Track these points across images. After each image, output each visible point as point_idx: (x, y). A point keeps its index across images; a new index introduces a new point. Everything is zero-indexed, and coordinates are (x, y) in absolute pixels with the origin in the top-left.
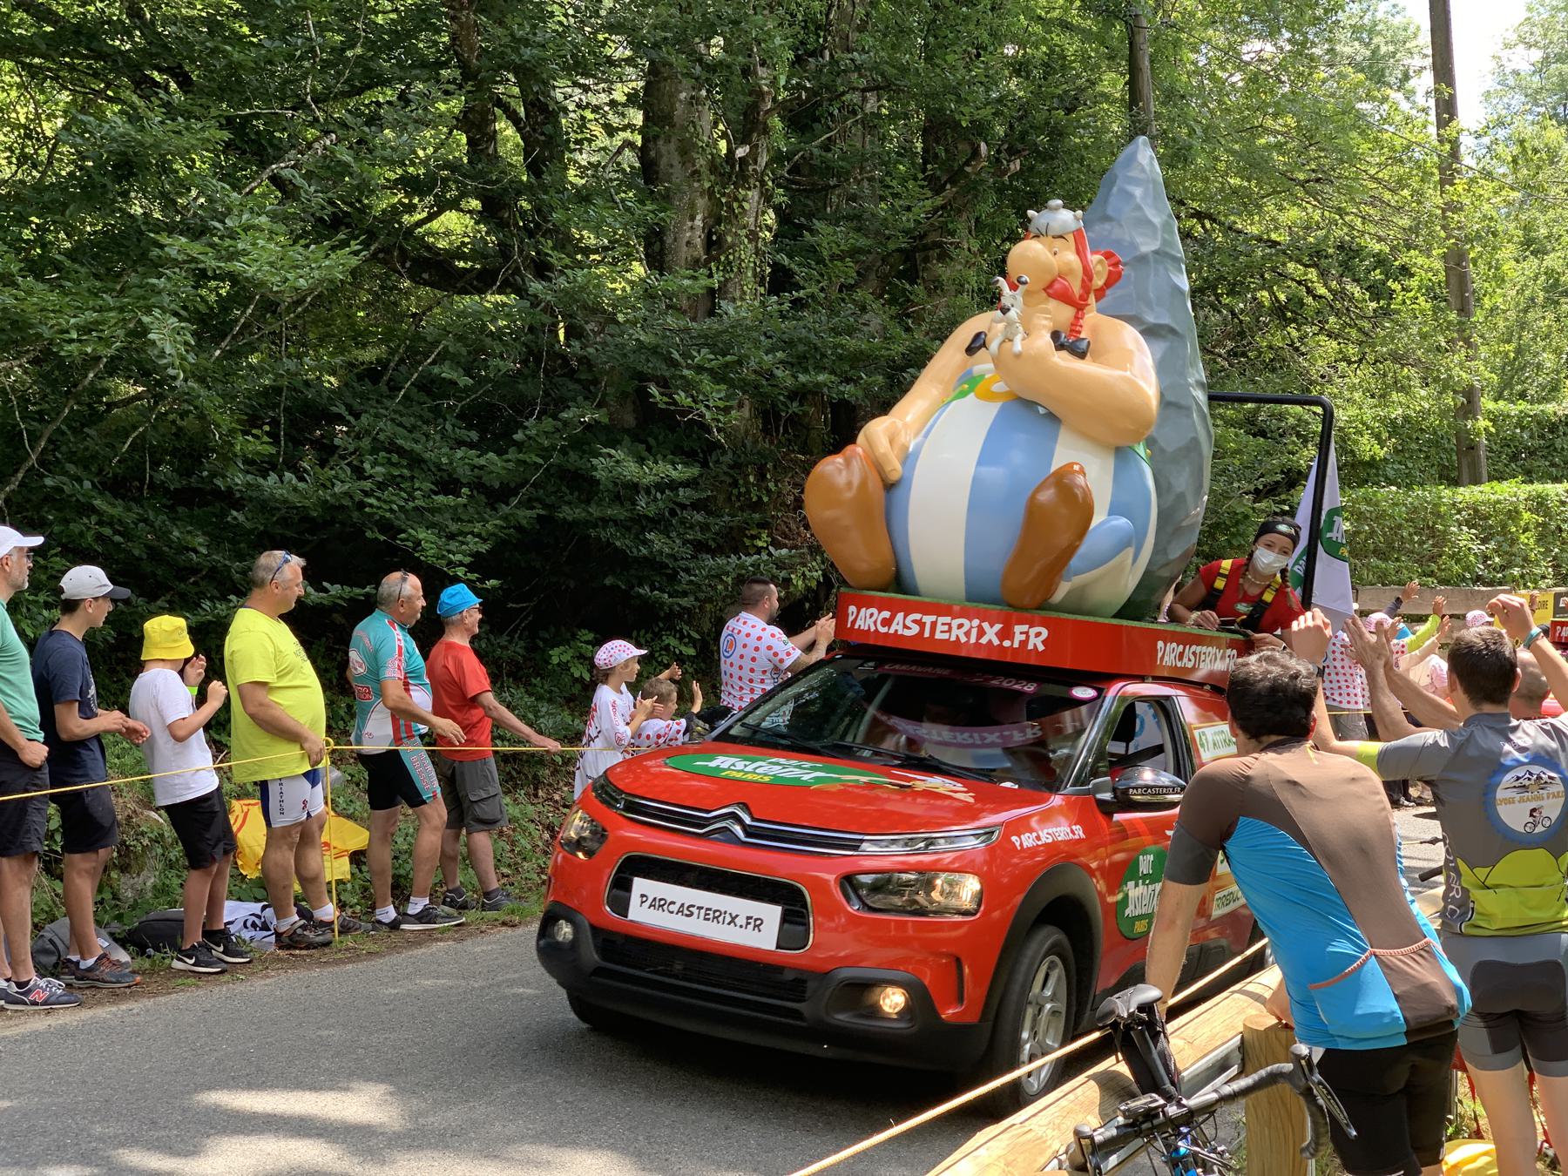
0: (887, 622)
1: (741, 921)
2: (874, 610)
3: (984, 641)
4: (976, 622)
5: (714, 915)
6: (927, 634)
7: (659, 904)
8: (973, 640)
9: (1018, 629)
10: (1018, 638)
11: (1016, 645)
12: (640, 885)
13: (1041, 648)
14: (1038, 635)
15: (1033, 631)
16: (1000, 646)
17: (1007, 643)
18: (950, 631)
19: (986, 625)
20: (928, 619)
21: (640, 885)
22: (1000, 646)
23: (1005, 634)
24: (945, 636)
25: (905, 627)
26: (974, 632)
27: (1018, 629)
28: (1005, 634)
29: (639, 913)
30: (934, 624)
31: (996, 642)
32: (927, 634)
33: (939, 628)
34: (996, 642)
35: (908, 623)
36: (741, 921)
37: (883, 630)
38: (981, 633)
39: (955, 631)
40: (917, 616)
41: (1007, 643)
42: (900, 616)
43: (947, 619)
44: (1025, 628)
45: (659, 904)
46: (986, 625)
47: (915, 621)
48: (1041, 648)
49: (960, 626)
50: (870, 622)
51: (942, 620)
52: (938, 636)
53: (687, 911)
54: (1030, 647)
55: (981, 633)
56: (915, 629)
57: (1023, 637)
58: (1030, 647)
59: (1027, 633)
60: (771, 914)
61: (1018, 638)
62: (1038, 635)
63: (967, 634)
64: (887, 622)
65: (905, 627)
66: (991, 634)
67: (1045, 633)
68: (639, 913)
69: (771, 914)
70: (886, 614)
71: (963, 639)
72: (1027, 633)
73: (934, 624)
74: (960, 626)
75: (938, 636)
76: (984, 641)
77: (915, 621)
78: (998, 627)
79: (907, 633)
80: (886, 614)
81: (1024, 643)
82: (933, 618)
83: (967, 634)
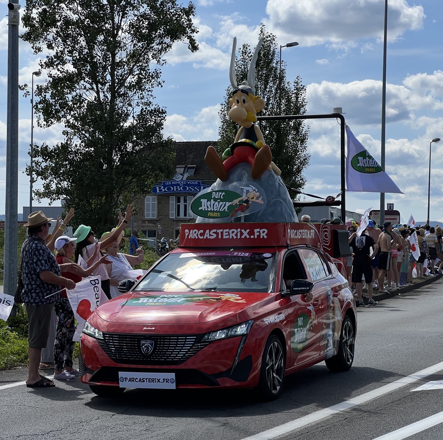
0: (201, 235)
2: (196, 230)
3: (243, 237)
4: (239, 230)
6: (220, 237)
8: (239, 237)
9: (256, 231)
10: (256, 234)
11: (256, 237)
13: (266, 237)
14: (264, 232)
15: (262, 231)
17: (252, 237)
18: (229, 234)
19: (243, 231)
20: (219, 231)
24: (228, 237)
25: (210, 235)
26: (239, 234)
27: (256, 231)
30: (222, 233)
31: (248, 237)
32: (220, 237)
33: (224, 234)
34: (248, 237)
35: (211, 233)
37: (202, 237)
38: (242, 234)
39: (231, 235)
40: (215, 230)
41: (252, 237)
42: (208, 231)
43: (227, 230)
44: (258, 230)
46: (243, 231)
48: (266, 237)
49: (233, 232)
50: (195, 235)
51: (225, 231)
52: (225, 237)
54: (261, 237)
56: (215, 236)
57: (258, 234)
58: (261, 237)
59: (259, 232)
61: (256, 234)
62: (264, 232)
63: (236, 235)
65: (210, 235)
66: (246, 234)
67: (266, 231)
70: (202, 231)
71: (235, 237)
72: (259, 232)
73: (222, 233)
74: (233, 232)
75: (225, 237)
76: (243, 237)
78: (248, 231)
79: (211, 237)
80: (202, 231)
82: (222, 230)
83: (236, 235)
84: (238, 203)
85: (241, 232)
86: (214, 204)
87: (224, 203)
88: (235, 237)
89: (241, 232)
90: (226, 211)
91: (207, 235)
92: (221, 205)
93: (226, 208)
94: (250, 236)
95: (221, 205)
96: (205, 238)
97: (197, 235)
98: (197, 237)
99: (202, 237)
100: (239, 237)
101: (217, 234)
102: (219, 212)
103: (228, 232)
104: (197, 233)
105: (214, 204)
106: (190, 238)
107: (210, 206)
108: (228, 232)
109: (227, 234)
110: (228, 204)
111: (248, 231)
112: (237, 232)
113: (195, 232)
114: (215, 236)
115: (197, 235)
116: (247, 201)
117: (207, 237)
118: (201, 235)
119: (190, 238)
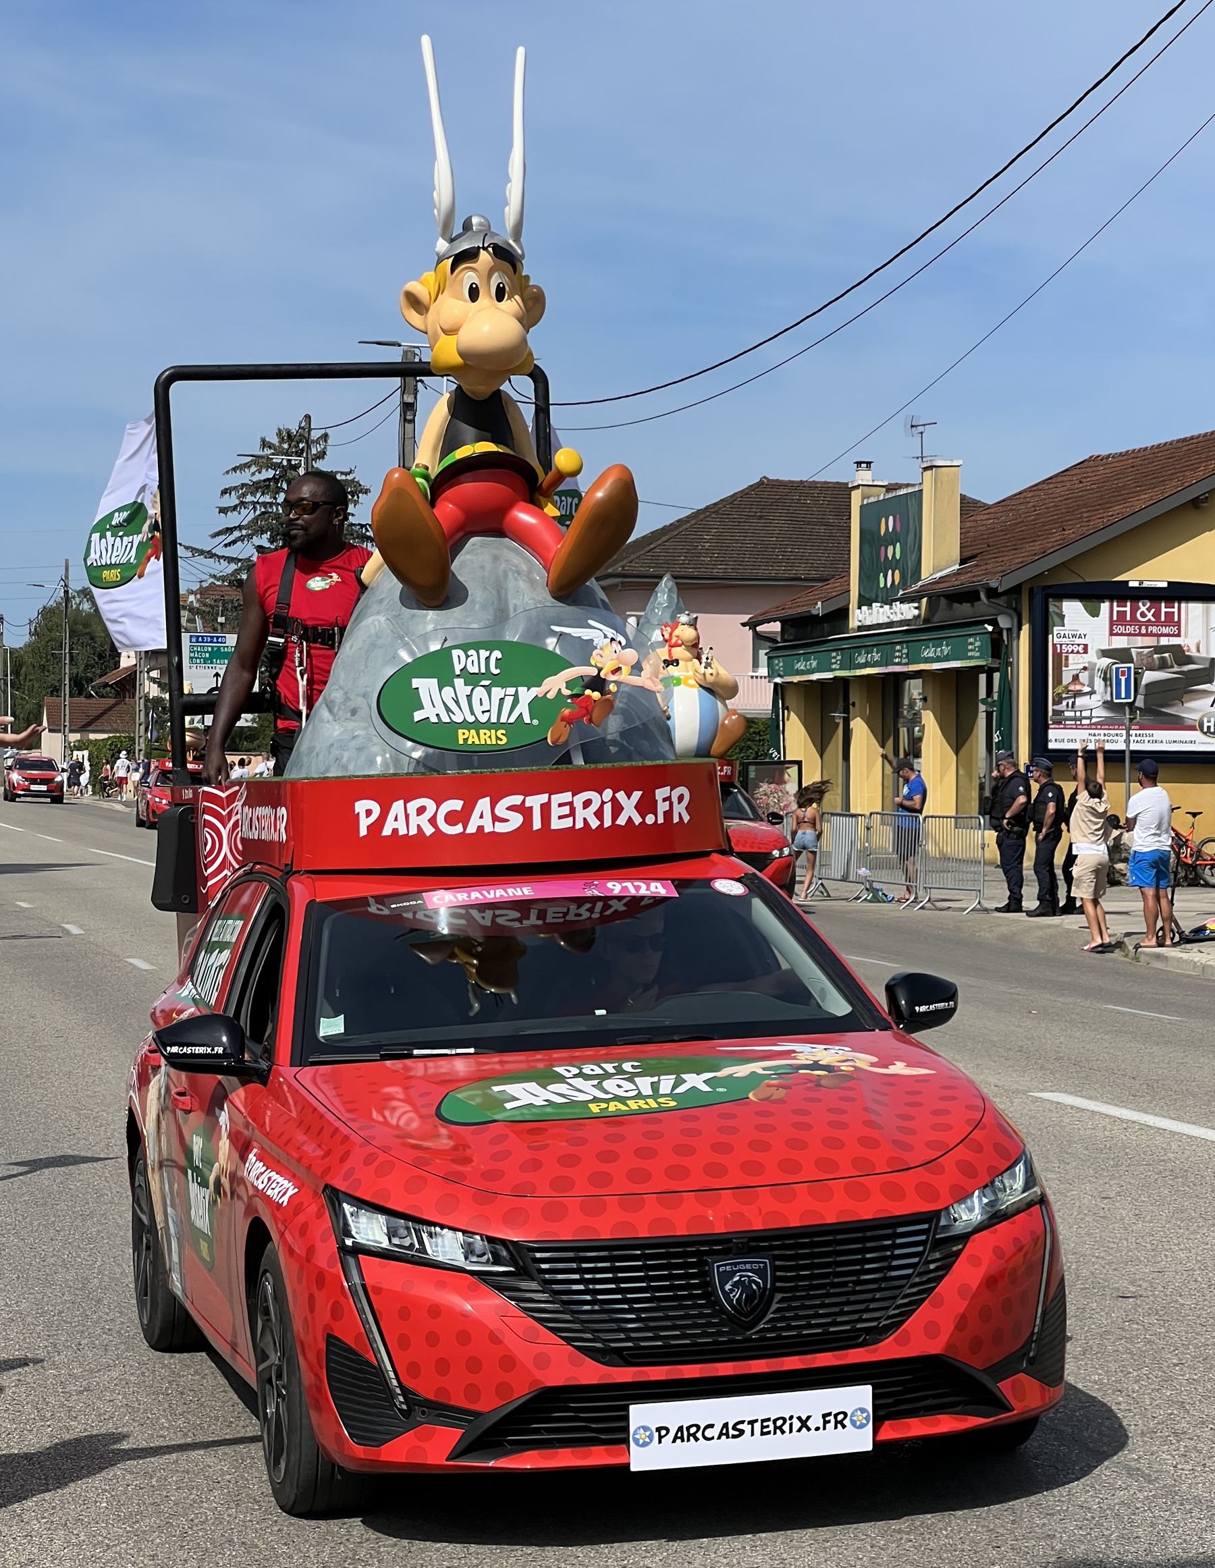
0: (451, 818)
2: (430, 804)
3: (621, 821)
4: (608, 794)
6: (537, 825)
8: (608, 823)
9: (661, 793)
11: (661, 820)
13: (686, 818)
16: (643, 822)
17: (650, 819)
18: (572, 813)
19: (621, 796)
20: (535, 802)
22: (643, 822)
24: (568, 823)
25: (496, 819)
26: (608, 808)
27: (661, 793)
28: (647, 806)
30: (546, 809)
31: (637, 820)
32: (537, 825)
33: (556, 811)
34: (637, 820)
37: (458, 829)
38: (617, 809)
39: (581, 813)
40: (516, 800)
41: (650, 819)
42: (484, 804)
43: (566, 797)
46: (621, 796)
47: (511, 808)
48: (686, 818)
49: (587, 804)
51: (557, 799)
52: (556, 824)
56: (516, 820)
57: (666, 806)
58: (676, 820)
61: (662, 807)
63: (599, 814)
65: (496, 819)
70: (456, 805)
71: (594, 823)
73: (546, 809)
74: (587, 804)
75: (556, 824)
76: (621, 821)
77: (510, 808)
78: (637, 795)
79: (501, 828)
80: (456, 805)
81: (668, 814)
82: (544, 798)
83: (599, 814)
84: (566, 692)
85: (614, 800)
86: (469, 697)
87: (511, 691)
88: (594, 823)
89: (614, 800)
90: (527, 720)
91: (482, 817)
92: (502, 700)
93: (523, 709)
94: (643, 817)
95: (502, 700)
96: (471, 829)
97: (433, 821)
98: (429, 830)
99: (458, 829)
100: (608, 823)
102: (497, 726)
103: (571, 804)
104: (428, 814)
105: (469, 697)
106: (387, 832)
107: (457, 702)
108: (571, 804)
109: (566, 810)
110: (527, 695)
111: (637, 795)
112: (603, 803)
113: (421, 810)
115: (433, 821)
117: (480, 828)
118: (451, 818)
119: (387, 832)
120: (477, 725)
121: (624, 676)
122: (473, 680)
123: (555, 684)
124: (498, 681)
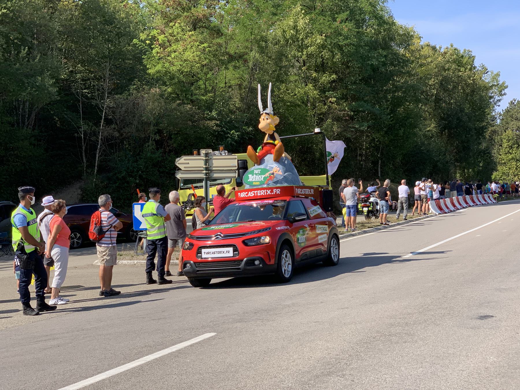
0: (247, 194)
1: (225, 252)
5: (220, 252)
7: (208, 253)
9: (274, 190)
10: (274, 192)
12: (203, 250)
20: (256, 192)
21: (203, 250)
23: (272, 192)
27: (274, 190)
28: (272, 192)
29: (204, 256)
36: (225, 252)
38: (267, 192)
45: (208, 253)
53: (214, 253)
55: (267, 192)
56: (253, 194)
60: (231, 249)
61: (274, 192)
64: (247, 194)
66: (269, 192)
67: (280, 190)
68: (204, 256)
69: (231, 249)
81: (276, 193)
91: (249, 195)
93: (262, 179)
101: (254, 193)
110: (263, 176)
114: (253, 194)
116: (273, 174)
120: (256, 181)
121: (277, 172)
122: (256, 174)
123: (267, 174)
124: (260, 174)
